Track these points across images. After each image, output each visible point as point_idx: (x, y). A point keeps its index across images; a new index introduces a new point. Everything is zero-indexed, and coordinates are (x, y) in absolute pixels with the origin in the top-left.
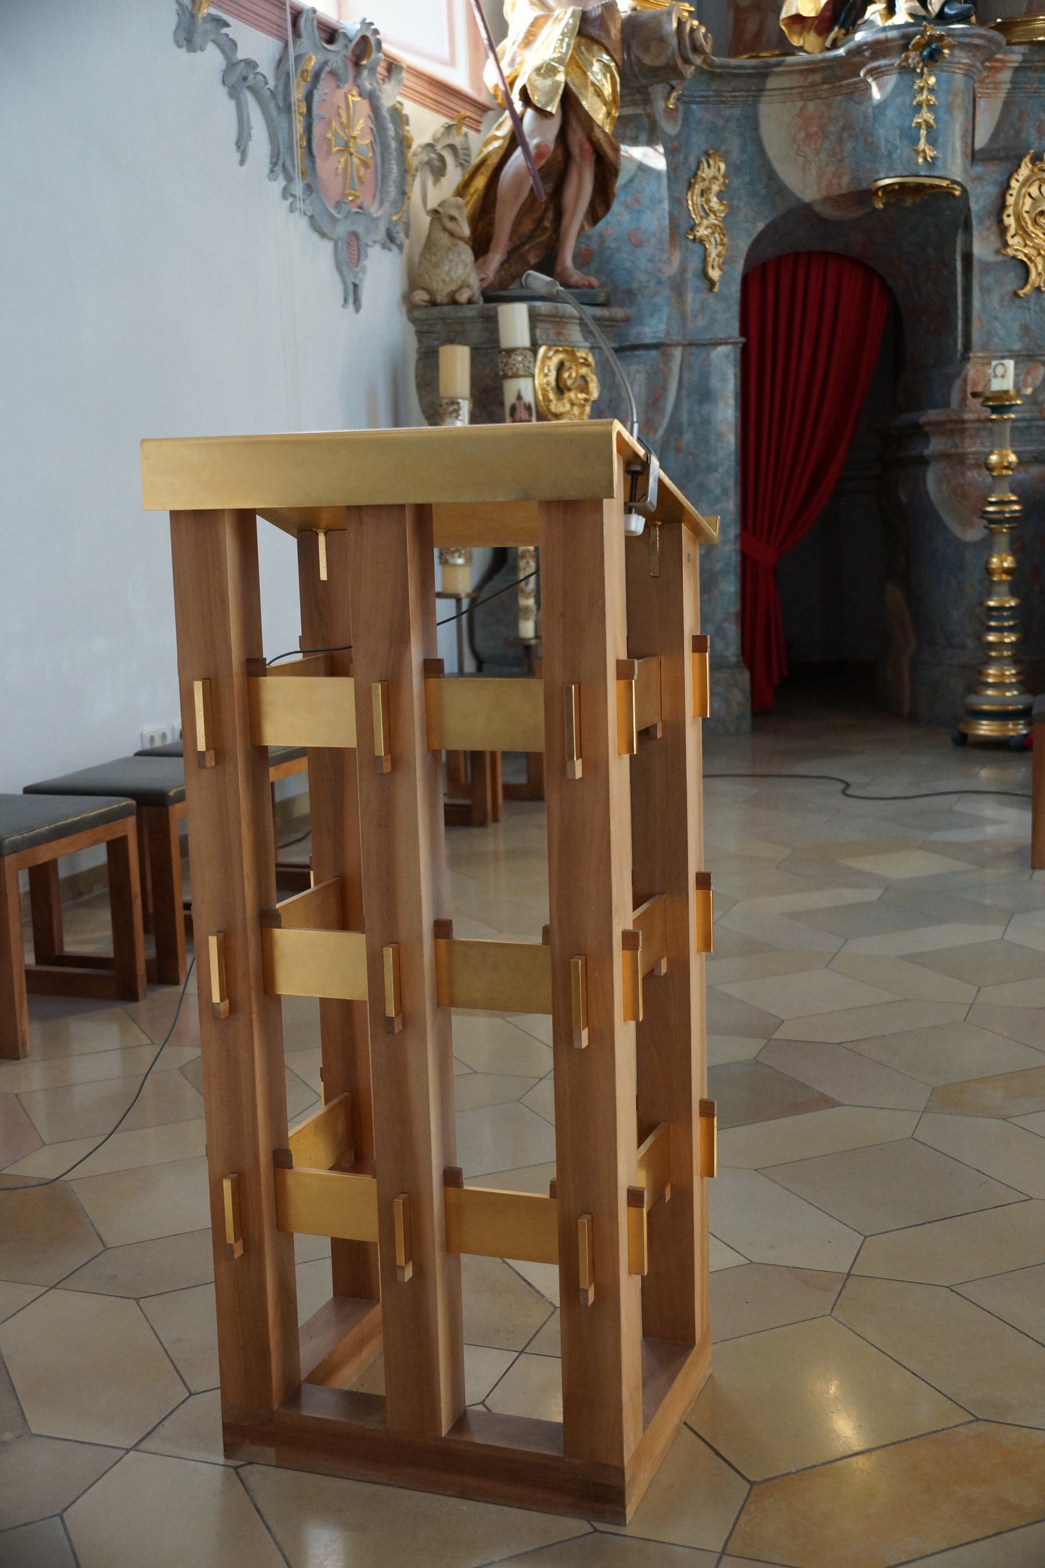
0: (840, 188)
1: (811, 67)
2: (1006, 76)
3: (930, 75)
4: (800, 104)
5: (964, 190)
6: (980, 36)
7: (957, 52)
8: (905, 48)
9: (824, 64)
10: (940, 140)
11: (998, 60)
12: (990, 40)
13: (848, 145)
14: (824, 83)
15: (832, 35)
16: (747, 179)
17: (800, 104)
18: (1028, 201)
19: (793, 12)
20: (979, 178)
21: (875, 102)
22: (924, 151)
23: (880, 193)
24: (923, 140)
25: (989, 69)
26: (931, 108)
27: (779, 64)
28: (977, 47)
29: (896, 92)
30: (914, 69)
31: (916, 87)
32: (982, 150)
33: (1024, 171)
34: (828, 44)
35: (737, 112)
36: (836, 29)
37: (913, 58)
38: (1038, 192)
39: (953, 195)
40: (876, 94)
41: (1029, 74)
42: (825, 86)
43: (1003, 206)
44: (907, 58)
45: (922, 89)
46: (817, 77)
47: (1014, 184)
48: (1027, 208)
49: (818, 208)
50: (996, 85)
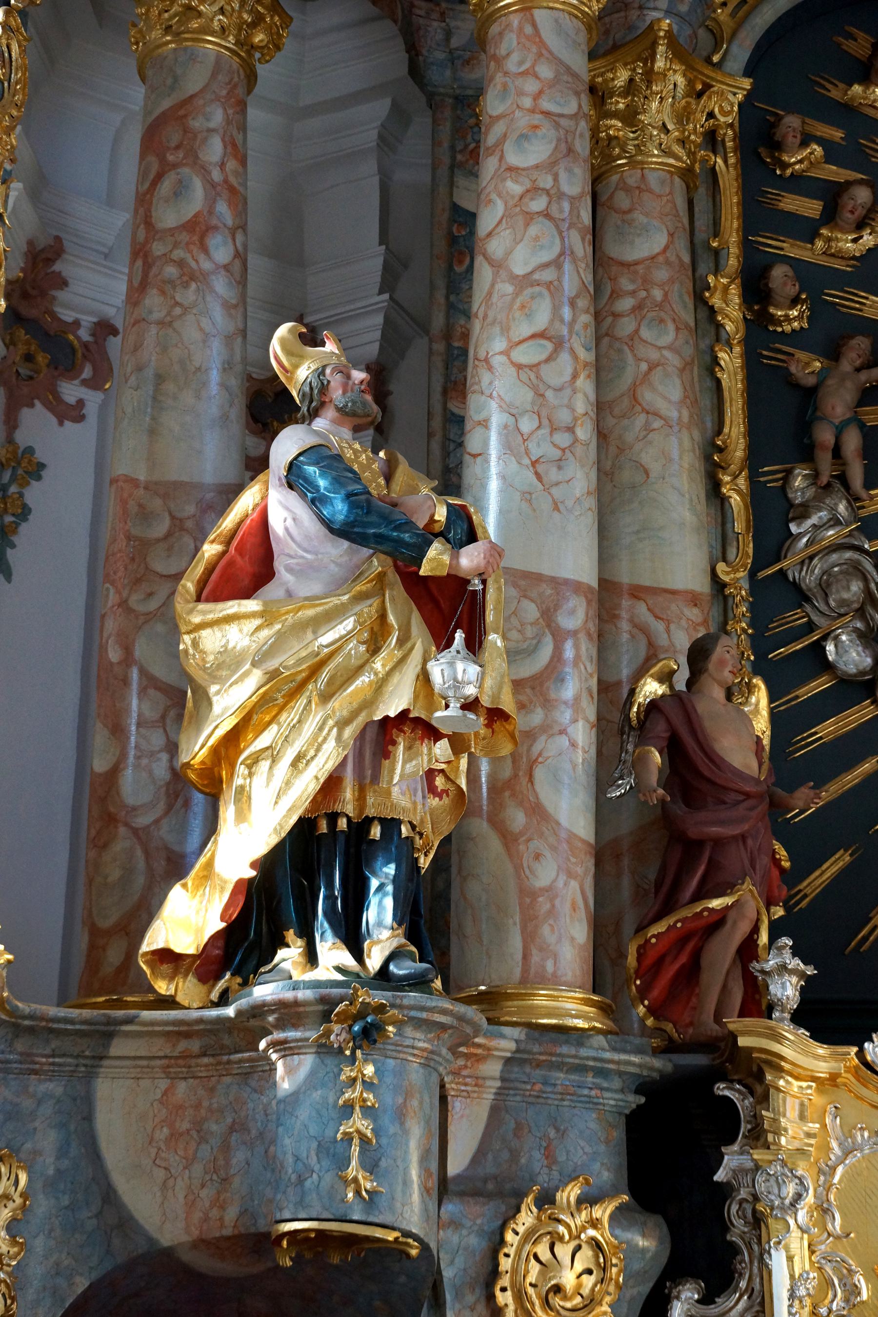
0: (222, 1226)
1: (184, 1028)
2: (493, 1068)
3: (366, 1061)
4: (164, 1084)
5: (425, 1247)
6: (444, 1012)
7: (409, 1031)
8: (326, 1017)
9: (201, 1027)
10: (383, 1163)
11: (479, 1046)
12: (461, 1018)
13: (239, 1156)
14: (204, 1055)
15: (221, 985)
16: (66, 1201)
17: (164, 1084)
18: (535, 1268)
19: (160, 945)
20: (455, 1224)
21: (280, 1094)
22: (355, 1180)
23: (285, 1243)
24: (354, 1163)
25: (467, 1056)
26: (368, 1111)
27: (130, 1021)
28: (443, 1027)
29: (312, 1082)
30: (341, 1050)
31: (343, 1077)
32: (458, 1177)
33: (526, 1219)
34: (214, 996)
35: (55, 1088)
36: (228, 976)
37: (338, 1033)
38: (548, 1255)
39: (408, 1256)
40: (285, 1084)
41: (528, 1069)
42: (206, 1060)
43: (494, 1273)
44: (327, 1034)
45: (354, 1080)
46: (195, 1045)
47: (509, 1237)
48: (532, 1278)
49: (187, 1257)
50: (479, 1081)
